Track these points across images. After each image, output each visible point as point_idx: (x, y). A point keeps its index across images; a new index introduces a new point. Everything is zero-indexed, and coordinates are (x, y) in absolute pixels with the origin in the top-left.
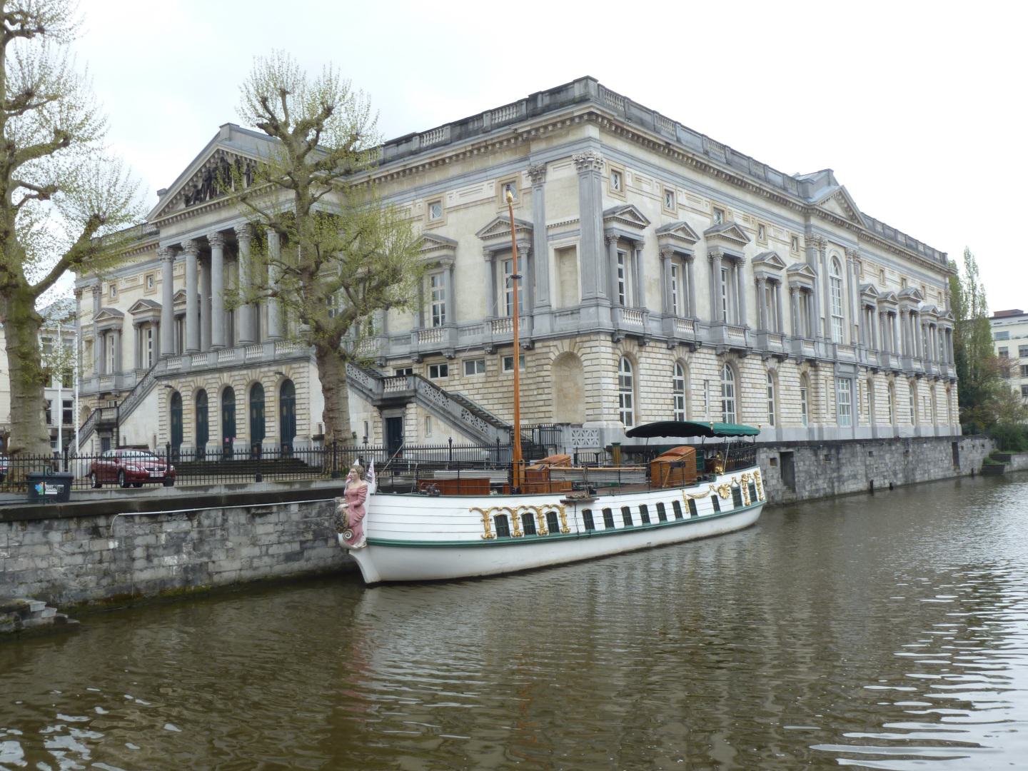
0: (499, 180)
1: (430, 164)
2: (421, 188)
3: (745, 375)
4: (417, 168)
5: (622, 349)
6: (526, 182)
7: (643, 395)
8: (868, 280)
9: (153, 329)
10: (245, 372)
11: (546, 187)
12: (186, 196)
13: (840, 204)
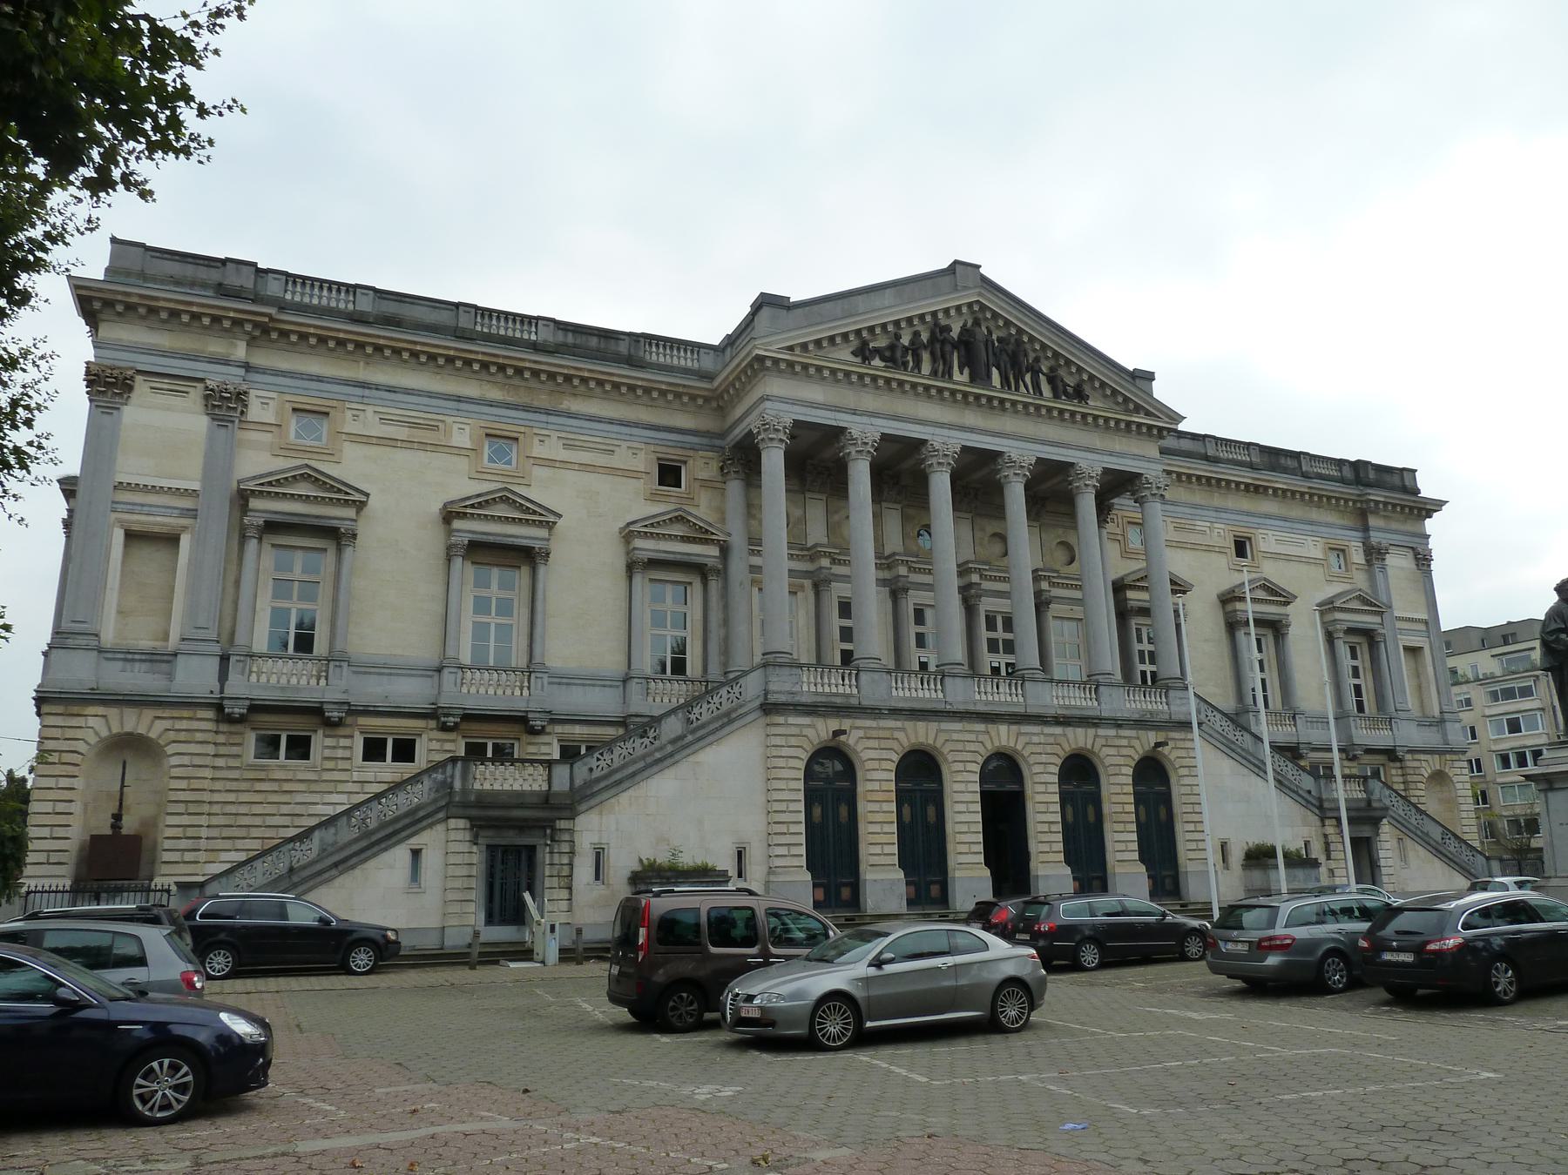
1: (1247, 485)
2: (1225, 510)
4: (1228, 482)
10: (1058, 730)
11: (1390, 571)
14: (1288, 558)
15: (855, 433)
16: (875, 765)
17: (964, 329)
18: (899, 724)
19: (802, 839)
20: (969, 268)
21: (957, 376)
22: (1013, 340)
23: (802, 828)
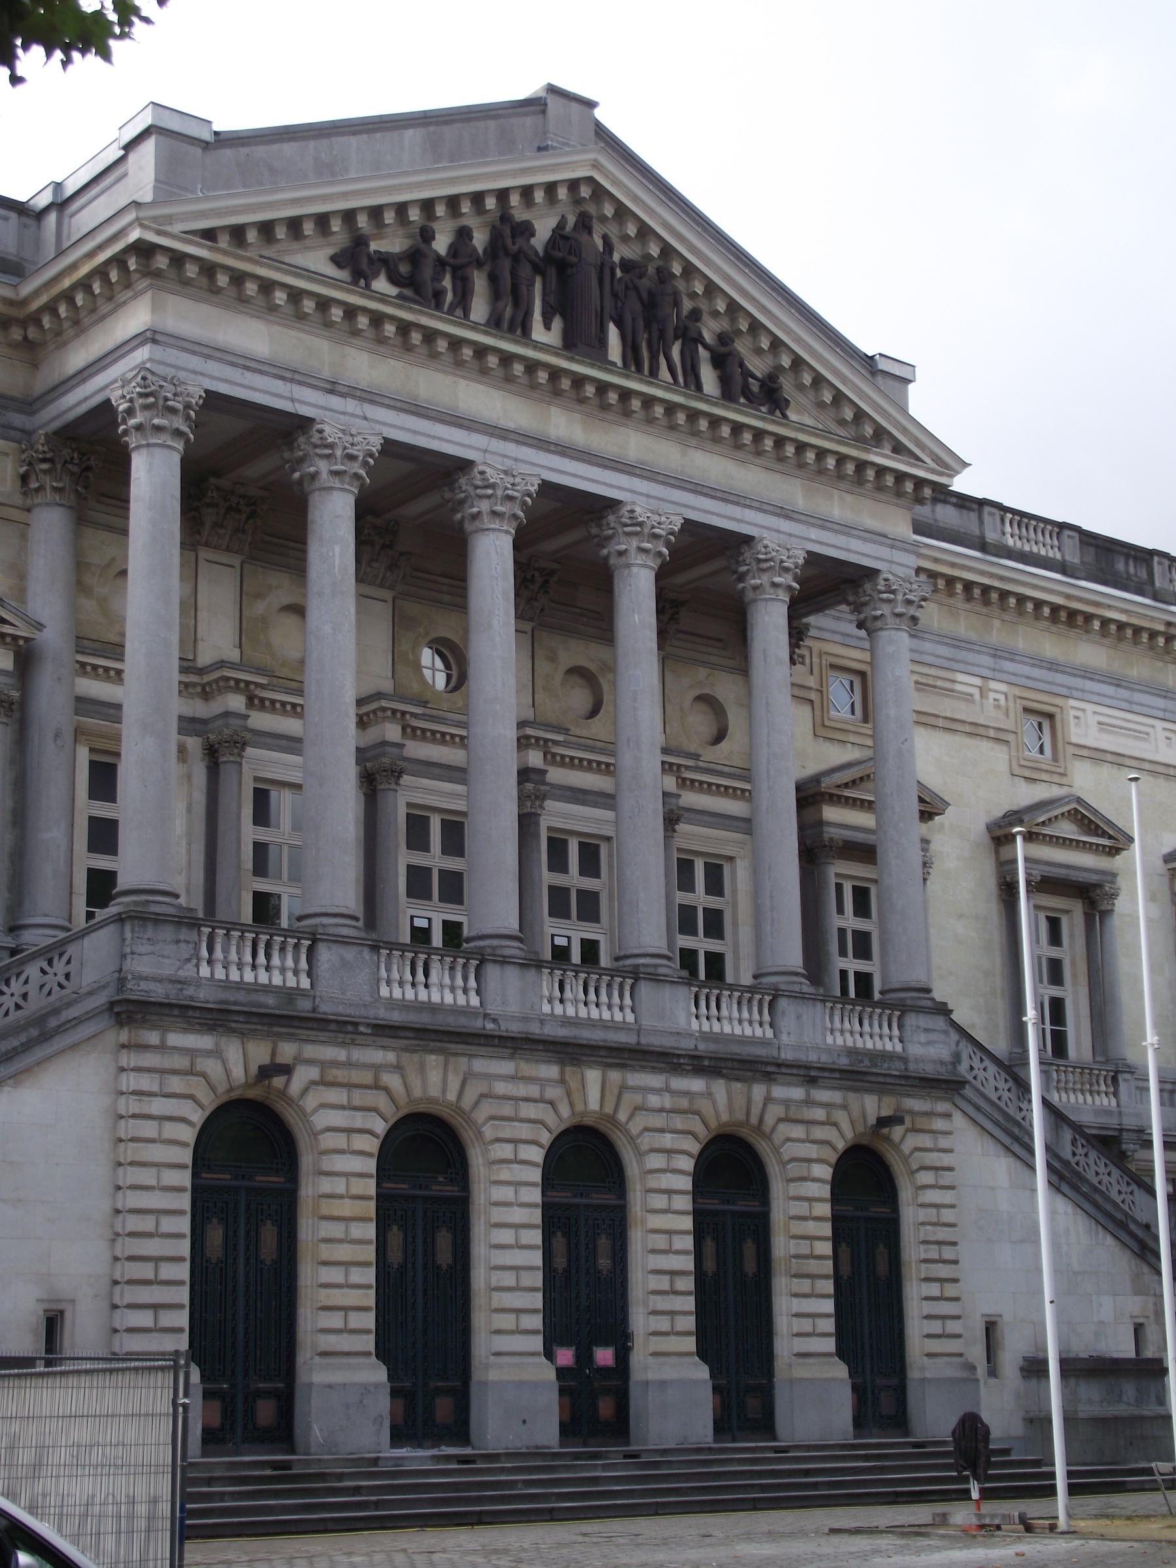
1: (1055, 609)
2: (1012, 655)
10: (697, 1084)
14: (1118, 760)
15: (331, 433)
16: (340, 1141)
17: (558, 235)
19: (183, 1295)
20: (574, 105)
21: (539, 333)
22: (651, 270)
23: (183, 1272)
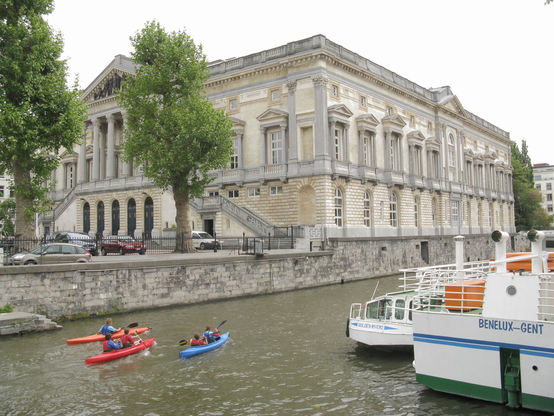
0: (270, 88)
1: (231, 79)
2: (226, 92)
3: (403, 199)
4: (224, 81)
5: (337, 184)
6: (285, 91)
7: (348, 209)
8: (468, 147)
9: (73, 167)
10: (125, 192)
11: (296, 93)
12: (95, 94)
13: (454, 105)
18: (95, 195)
